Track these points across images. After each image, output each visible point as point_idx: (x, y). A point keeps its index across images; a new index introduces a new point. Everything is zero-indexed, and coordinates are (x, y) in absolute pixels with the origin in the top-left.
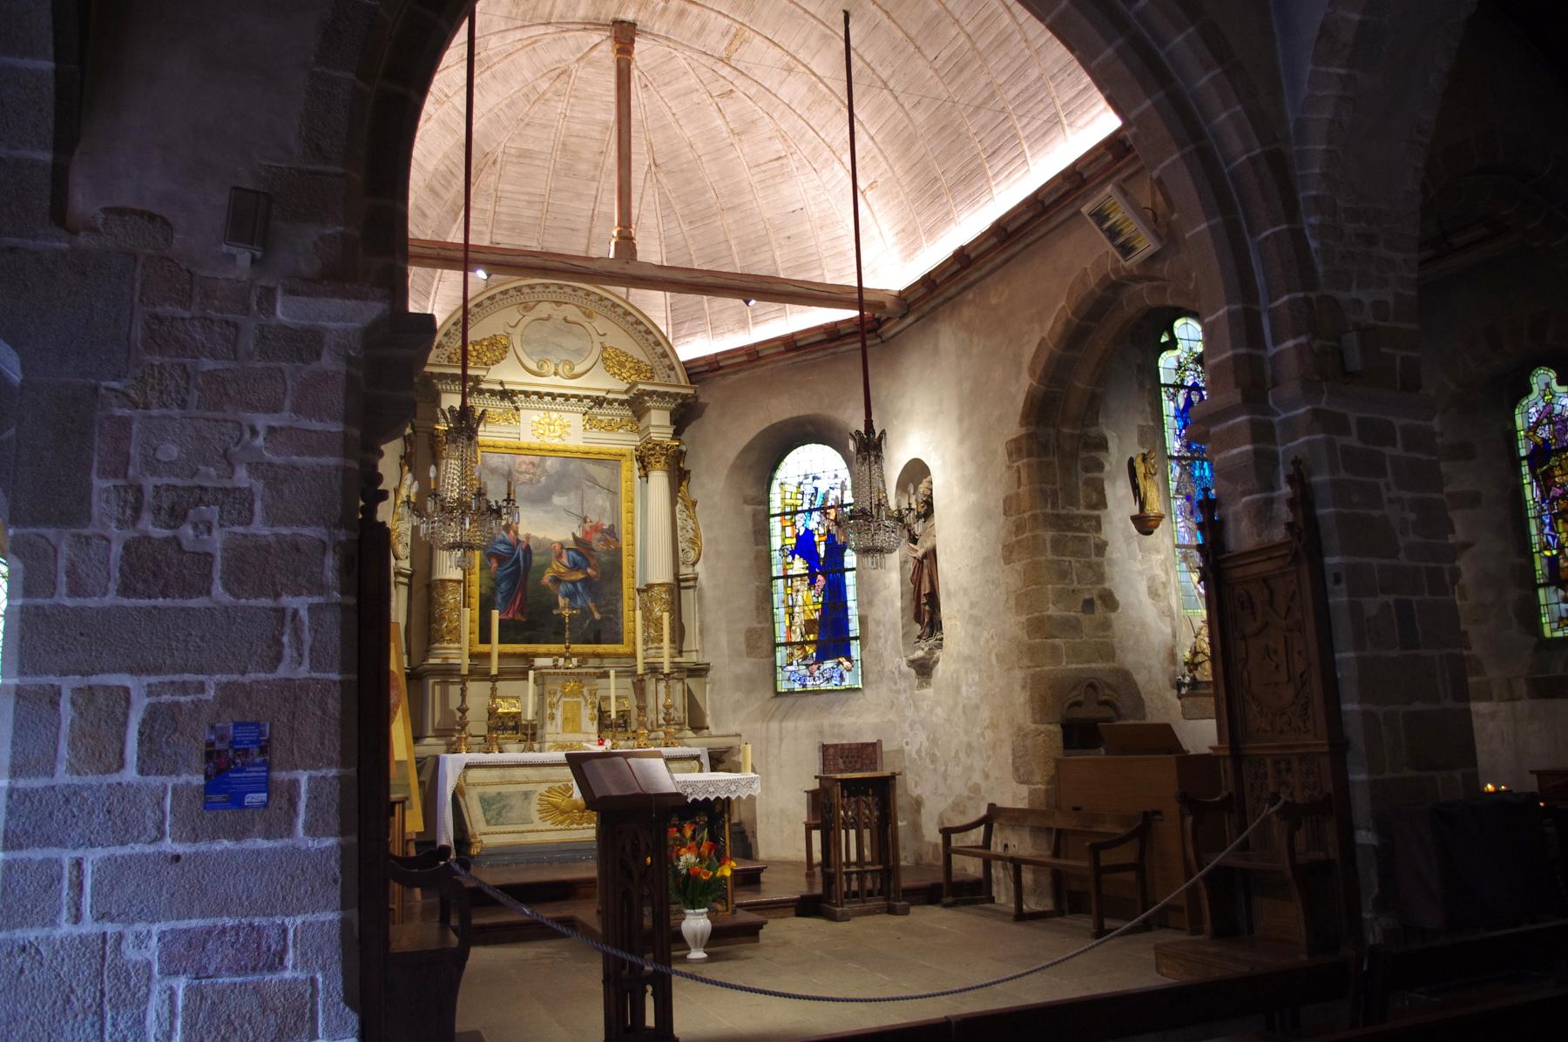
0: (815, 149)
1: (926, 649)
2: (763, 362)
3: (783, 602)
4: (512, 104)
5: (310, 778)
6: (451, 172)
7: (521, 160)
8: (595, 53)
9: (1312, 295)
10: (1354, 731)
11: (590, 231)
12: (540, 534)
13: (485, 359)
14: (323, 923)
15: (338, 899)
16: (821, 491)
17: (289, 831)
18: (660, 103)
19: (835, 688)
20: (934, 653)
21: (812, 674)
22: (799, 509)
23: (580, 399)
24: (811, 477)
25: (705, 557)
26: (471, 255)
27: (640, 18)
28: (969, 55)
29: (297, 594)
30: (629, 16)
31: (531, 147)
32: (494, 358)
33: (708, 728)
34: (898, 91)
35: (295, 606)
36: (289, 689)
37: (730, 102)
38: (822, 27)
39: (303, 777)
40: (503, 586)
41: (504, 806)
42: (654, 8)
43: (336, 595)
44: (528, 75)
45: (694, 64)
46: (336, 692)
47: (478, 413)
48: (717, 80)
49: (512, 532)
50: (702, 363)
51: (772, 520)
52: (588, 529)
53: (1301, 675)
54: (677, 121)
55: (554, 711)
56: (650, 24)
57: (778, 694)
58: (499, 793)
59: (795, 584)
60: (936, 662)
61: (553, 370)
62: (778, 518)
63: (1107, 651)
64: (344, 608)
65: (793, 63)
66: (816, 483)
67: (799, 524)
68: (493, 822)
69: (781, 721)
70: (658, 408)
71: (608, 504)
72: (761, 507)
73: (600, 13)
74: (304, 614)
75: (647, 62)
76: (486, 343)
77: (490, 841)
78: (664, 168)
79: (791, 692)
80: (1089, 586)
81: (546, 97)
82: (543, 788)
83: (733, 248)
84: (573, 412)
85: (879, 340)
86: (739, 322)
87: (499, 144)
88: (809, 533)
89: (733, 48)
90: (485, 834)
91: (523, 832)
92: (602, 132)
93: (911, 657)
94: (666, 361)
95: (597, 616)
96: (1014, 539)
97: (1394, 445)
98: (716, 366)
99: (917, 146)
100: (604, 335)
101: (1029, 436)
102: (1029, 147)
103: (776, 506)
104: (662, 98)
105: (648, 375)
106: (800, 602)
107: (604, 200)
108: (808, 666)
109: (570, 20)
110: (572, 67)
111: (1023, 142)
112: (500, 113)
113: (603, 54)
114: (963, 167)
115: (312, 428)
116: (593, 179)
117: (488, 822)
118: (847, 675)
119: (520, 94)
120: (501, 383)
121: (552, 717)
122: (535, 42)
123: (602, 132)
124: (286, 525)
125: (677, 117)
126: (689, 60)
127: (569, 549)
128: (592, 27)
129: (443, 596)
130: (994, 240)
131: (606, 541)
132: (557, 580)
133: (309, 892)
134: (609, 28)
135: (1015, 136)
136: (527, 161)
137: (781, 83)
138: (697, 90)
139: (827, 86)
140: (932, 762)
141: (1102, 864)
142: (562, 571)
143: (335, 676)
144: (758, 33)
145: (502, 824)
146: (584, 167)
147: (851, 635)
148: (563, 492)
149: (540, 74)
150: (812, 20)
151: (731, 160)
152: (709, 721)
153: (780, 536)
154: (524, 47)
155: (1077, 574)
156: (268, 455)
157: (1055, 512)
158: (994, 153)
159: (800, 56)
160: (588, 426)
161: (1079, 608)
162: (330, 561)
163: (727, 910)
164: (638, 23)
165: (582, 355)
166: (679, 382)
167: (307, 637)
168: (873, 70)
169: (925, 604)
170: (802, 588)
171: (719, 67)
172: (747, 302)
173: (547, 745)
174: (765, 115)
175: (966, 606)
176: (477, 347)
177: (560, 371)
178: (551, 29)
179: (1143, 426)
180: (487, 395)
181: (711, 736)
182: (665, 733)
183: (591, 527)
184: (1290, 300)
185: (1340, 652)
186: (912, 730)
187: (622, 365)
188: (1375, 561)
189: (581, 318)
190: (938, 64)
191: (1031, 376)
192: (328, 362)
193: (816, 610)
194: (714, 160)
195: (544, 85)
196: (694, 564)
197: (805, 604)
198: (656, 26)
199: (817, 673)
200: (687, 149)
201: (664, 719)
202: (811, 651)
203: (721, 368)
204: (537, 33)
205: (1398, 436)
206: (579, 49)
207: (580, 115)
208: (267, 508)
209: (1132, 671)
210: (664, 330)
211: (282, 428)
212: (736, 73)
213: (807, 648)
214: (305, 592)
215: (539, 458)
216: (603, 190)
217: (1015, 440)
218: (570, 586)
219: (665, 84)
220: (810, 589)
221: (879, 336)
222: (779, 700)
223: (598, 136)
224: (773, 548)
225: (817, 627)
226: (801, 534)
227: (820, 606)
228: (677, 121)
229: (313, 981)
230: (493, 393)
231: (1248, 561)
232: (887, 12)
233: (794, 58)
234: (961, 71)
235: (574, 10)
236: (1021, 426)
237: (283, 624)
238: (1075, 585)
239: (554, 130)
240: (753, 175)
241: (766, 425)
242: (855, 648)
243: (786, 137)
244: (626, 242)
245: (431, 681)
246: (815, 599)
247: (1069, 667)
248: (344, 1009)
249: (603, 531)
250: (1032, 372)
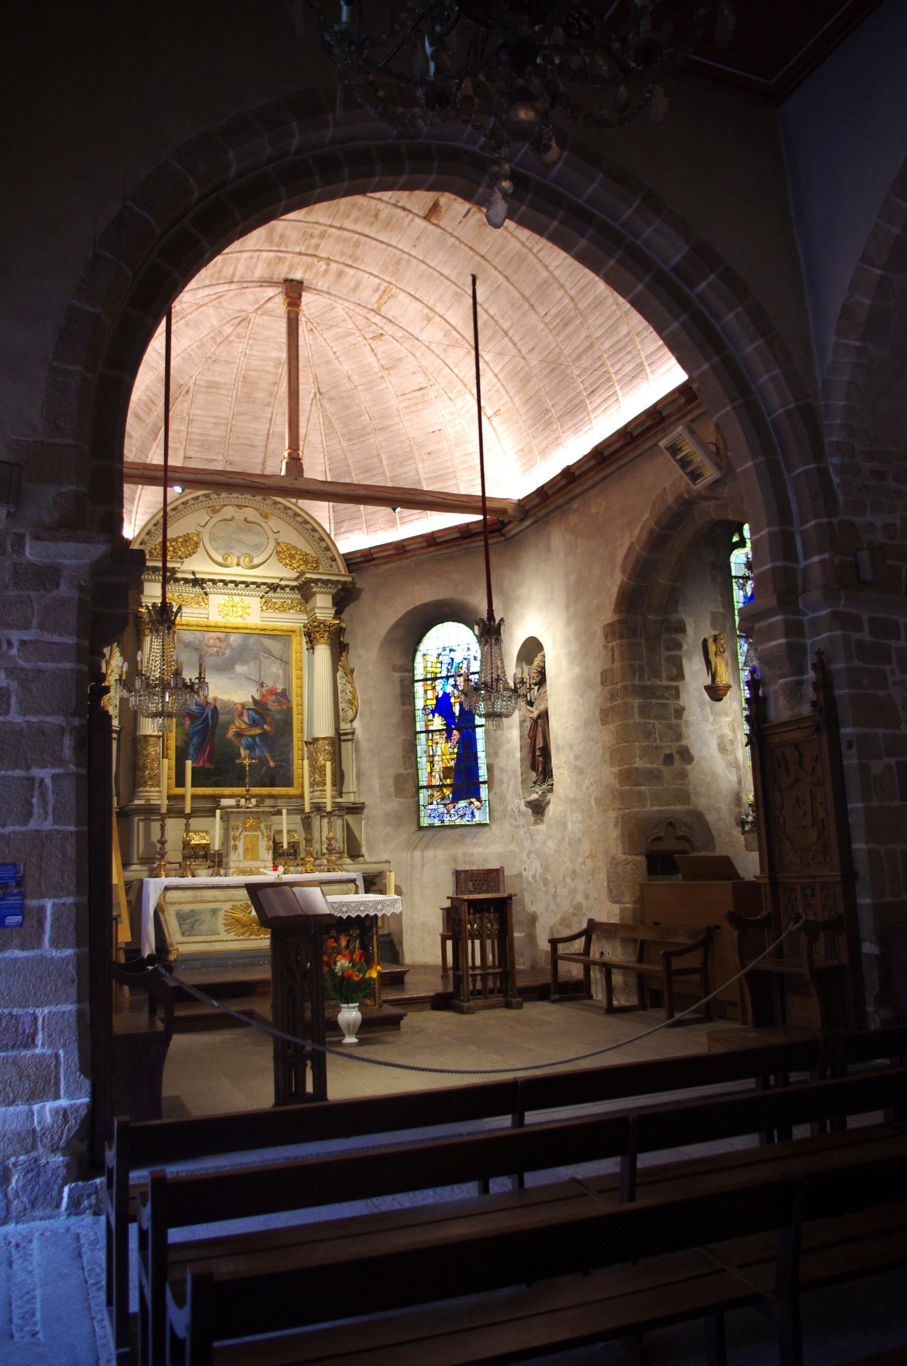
0: (450, 382)
1: (540, 793)
2: (408, 555)
3: (425, 752)
4: (202, 345)
5: (54, 905)
6: (152, 401)
7: (209, 390)
8: (269, 305)
9: (835, 520)
10: (862, 866)
11: (266, 447)
13: (180, 553)
14: (64, 1012)
15: (75, 995)
16: (456, 661)
17: (39, 944)
18: (323, 343)
19: (467, 823)
20: (546, 796)
21: (448, 812)
22: (439, 675)
23: (258, 585)
24: (448, 649)
25: (361, 715)
26: (170, 474)
27: (306, 277)
28: (573, 313)
29: (43, 766)
30: (297, 275)
31: (217, 379)
32: (187, 552)
33: (363, 856)
34: (516, 339)
35: (42, 776)
36: (40, 839)
37: (380, 343)
38: (454, 287)
39: (49, 904)
40: (195, 739)
41: (196, 921)
42: (318, 270)
43: (72, 767)
44: (215, 322)
45: (351, 313)
46: (73, 840)
47: (175, 610)
48: (370, 326)
50: (358, 555)
51: (416, 684)
52: (265, 693)
53: (822, 821)
54: (337, 358)
56: (315, 282)
57: (421, 828)
58: (192, 910)
59: (435, 737)
60: (548, 803)
61: (235, 562)
62: (421, 683)
63: (684, 796)
64: (78, 776)
65: (431, 314)
66: (452, 655)
67: (438, 688)
68: (187, 933)
69: (423, 850)
70: (322, 593)
71: (281, 671)
72: (407, 674)
73: (273, 274)
74: (48, 781)
75: (312, 311)
76: (180, 540)
77: (185, 949)
78: (327, 396)
79: (431, 827)
80: (670, 744)
81: (230, 339)
82: (228, 906)
83: (384, 461)
84: (252, 596)
85: (503, 538)
86: (389, 521)
87: (191, 377)
88: (446, 696)
89: (382, 301)
90: (180, 943)
91: (211, 942)
92: (275, 367)
93: (528, 799)
94: (329, 554)
95: (272, 764)
96: (609, 705)
97: (899, 639)
98: (369, 557)
99: (532, 383)
100: (278, 532)
101: (620, 622)
102: (621, 388)
103: (419, 674)
104: (325, 339)
105: (314, 565)
106: (439, 753)
107: (278, 422)
108: (445, 805)
109: (249, 280)
110: (251, 315)
111: (616, 384)
112: (192, 353)
113: (277, 305)
114: (569, 402)
115: (53, 641)
116: (269, 404)
117: (183, 934)
118: (477, 813)
119: (209, 337)
120: (193, 573)
121: (235, 848)
122: (220, 297)
123: (275, 367)
124: (34, 715)
125: (337, 354)
126: (347, 310)
127: (248, 709)
128: (267, 284)
129: (146, 749)
130: (593, 462)
131: (279, 702)
132: (239, 735)
133: (53, 990)
134: (281, 285)
135: (609, 379)
136: (214, 390)
137: (422, 329)
138: (354, 334)
139: (459, 333)
140: (545, 885)
141: (673, 968)
142: (243, 727)
143: (72, 828)
144: (403, 290)
145: (195, 935)
146: (261, 395)
147: (481, 780)
148: (244, 662)
149: (225, 321)
150: (446, 281)
151: (381, 390)
152: (364, 850)
153: (423, 698)
154: (211, 301)
155: (659, 734)
156: (21, 662)
157: (642, 683)
158: (593, 391)
159: (437, 309)
160: (264, 608)
161: (661, 761)
162: (68, 741)
163: (375, 1005)
164: (305, 281)
165: (259, 549)
166: (340, 571)
167: (51, 798)
168: (496, 321)
169: (539, 756)
170: (440, 741)
171: (371, 315)
172: (394, 510)
173: (231, 871)
174: (410, 355)
175: (572, 758)
176: (173, 544)
177: (242, 562)
178: (234, 286)
179: (715, 613)
180: (182, 582)
181: (365, 863)
182: (328, 861)
183: (267, 691)
184: (816, 525)
185: (851, 803)
186: (529, 859)
187: (292, 557)
188: (880, 731)
189: (259, 519)
190: (548, 319)
191: (623, 573)
192: (65, 590)
193: (452, 759)
194: (368, 389)
195: (228, 330)
196: (352, 721)
197: (443, 754)
198: (320, 284)
199: (452, 811)
200: (346, 380)
201: (327, 849)
202: (448, 793)
203: (374, 559)
204: (222, 290)
205: (902, 632)
206: (256, 301)
207: (258, 353)
208: (20, 702)
209: (704, 812)
210: (326, 527)
211: (30, 641)
212: (385, 320)
213: (445, 790)
214: (49, 765)
215: (224, 634)
216: (277, 413)
217: (610, 625)
218: (250, 739)
219: (327, 329)
220: (447, 742)
221: (503, 535)
222: (421, 833)
223: (271, 369)
224: (417, 708)
225: (453, 773)
226: (440, 696)
227: (455, 756)
228: (337, 358)
229: (57, 1056)
230: (186, 581)
231: (782, 730)
232: (506, 277)
233: (432, 310)
234: (566, 325)
235: (252, 272)
236: (615, 612)
237: (33, 790)
238: (658, 743)
239: (236, 366)
240: (400, 402)
241: (411, 607)
242: (484, 791)
243: (427, 372)
244: (295, 462)
245: (136, 819)
246: (451, 750)
247: (653, 809)
248: (80, 1076)
249: (276, 694)
250: (623, 571)
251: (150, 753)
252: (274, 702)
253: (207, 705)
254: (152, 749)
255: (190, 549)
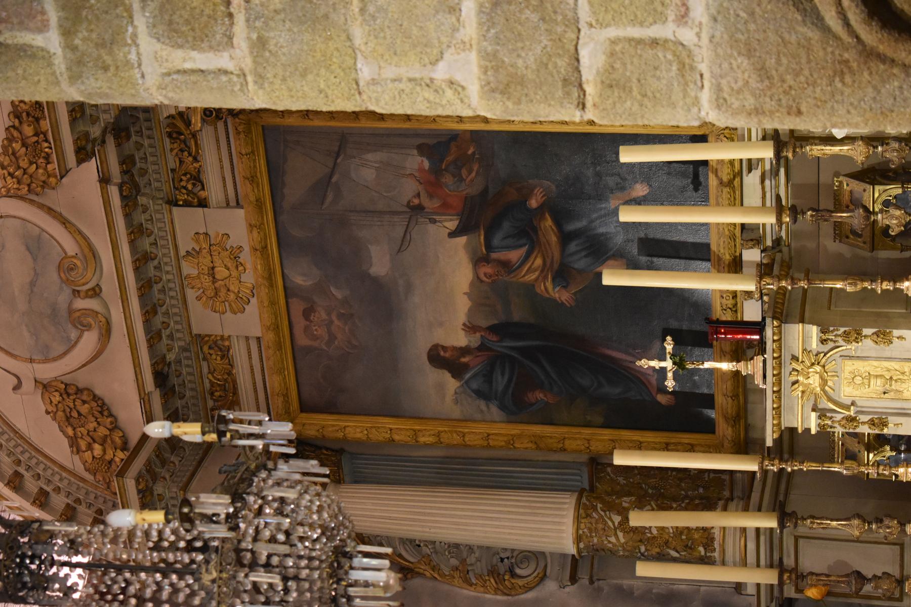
12: (462, 306)
23: (136, 232)
40: (585, 381)
49: (464, 360)
52: (436, 203)
55: (864, 418)
71: (370, 156)
127: (489, 247)
142: (539, 262)
176: (83, 445)
183: (431, 196)
218: (573, 247)
249: (436, 171)
251: (622, 545)
252: (462, 180)
253: (489, 349)
254: (613, 539)
255: (84, 409)
